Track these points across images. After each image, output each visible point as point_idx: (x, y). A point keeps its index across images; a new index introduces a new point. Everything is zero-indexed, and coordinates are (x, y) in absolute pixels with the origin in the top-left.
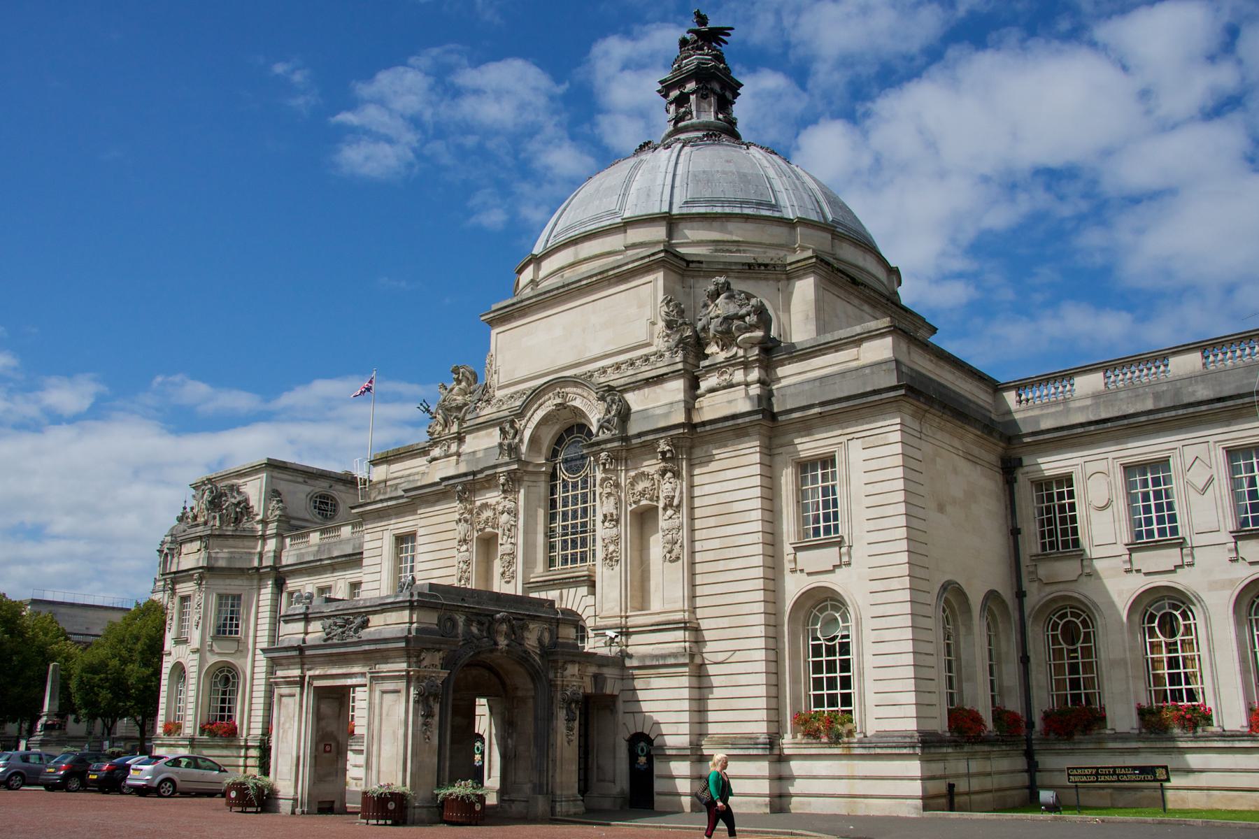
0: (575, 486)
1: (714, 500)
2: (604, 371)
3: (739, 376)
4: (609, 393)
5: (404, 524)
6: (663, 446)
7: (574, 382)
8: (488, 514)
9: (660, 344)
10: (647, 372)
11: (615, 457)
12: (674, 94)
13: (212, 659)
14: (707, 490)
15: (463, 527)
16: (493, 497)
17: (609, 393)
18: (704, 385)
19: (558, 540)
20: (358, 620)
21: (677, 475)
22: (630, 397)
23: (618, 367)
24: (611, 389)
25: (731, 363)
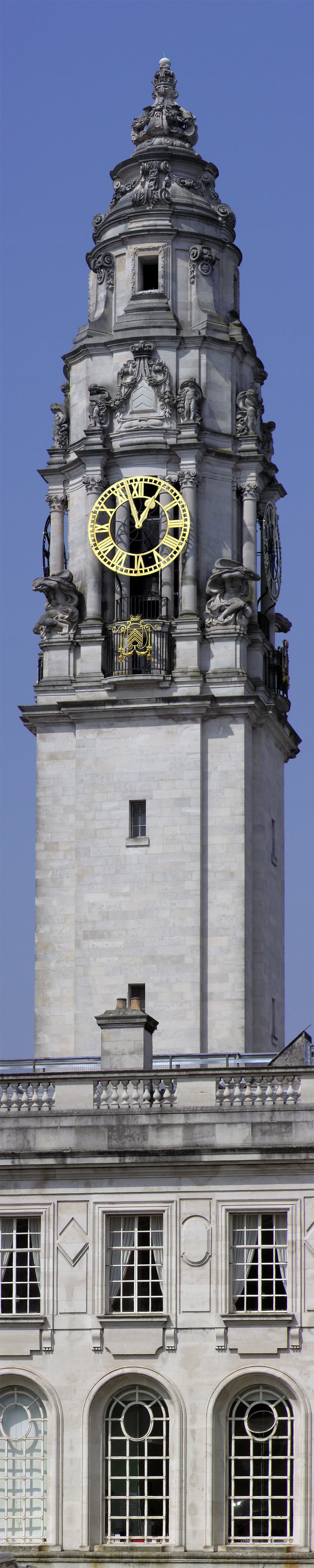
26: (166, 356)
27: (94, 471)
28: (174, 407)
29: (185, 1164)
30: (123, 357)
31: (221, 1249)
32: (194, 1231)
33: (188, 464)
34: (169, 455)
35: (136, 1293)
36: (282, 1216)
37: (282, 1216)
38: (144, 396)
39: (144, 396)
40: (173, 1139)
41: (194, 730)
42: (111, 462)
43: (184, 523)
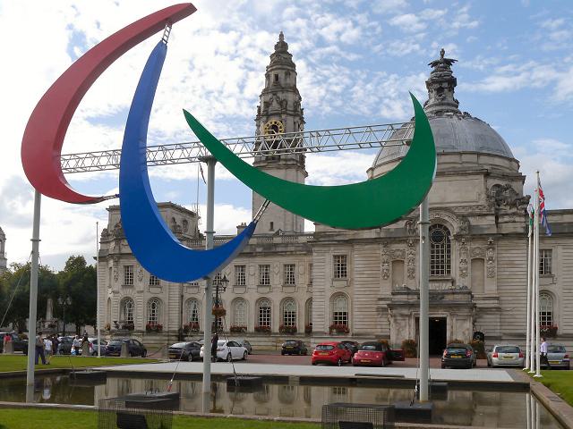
0: (438, 247)
1: (507, 259)
2: (457, 207)
3: (517, 219)
4: (464, 218)
5: (342, 251)
6: (491, 240)
7: (446, 209)
8: (398, 253)
9: (483, 201)
10: (477, 211)
11: (467, 240)
12: (437, 86)
13: (150, 296)
14: (504, 255)
15: (385, 258)
16: (402, 246)
17: (464, 218)
18: (500, 220)
19: (445, 267)
20: (440, 296)
21: (494, 249)
22: (470, 219)
23: (464, 207)
24: (463, 216)
25: (514, 214)
26: (280, 95)
27: (265, 118)
28: (281, 106)
29: (250, 255)
30: (270, 96)
31: (257, 272)
32: (252, 269)
33: (283, 116)
34: (279, 115)
35: (265, 282)
36: (269, 266)
37: (269, 266)
38: (275, 103)
39: (275, 103)
40: (248, 251)
41: (284, 171)
42: (268, 116)
43: (283, 129)
